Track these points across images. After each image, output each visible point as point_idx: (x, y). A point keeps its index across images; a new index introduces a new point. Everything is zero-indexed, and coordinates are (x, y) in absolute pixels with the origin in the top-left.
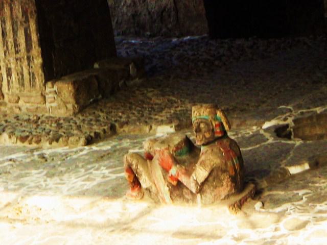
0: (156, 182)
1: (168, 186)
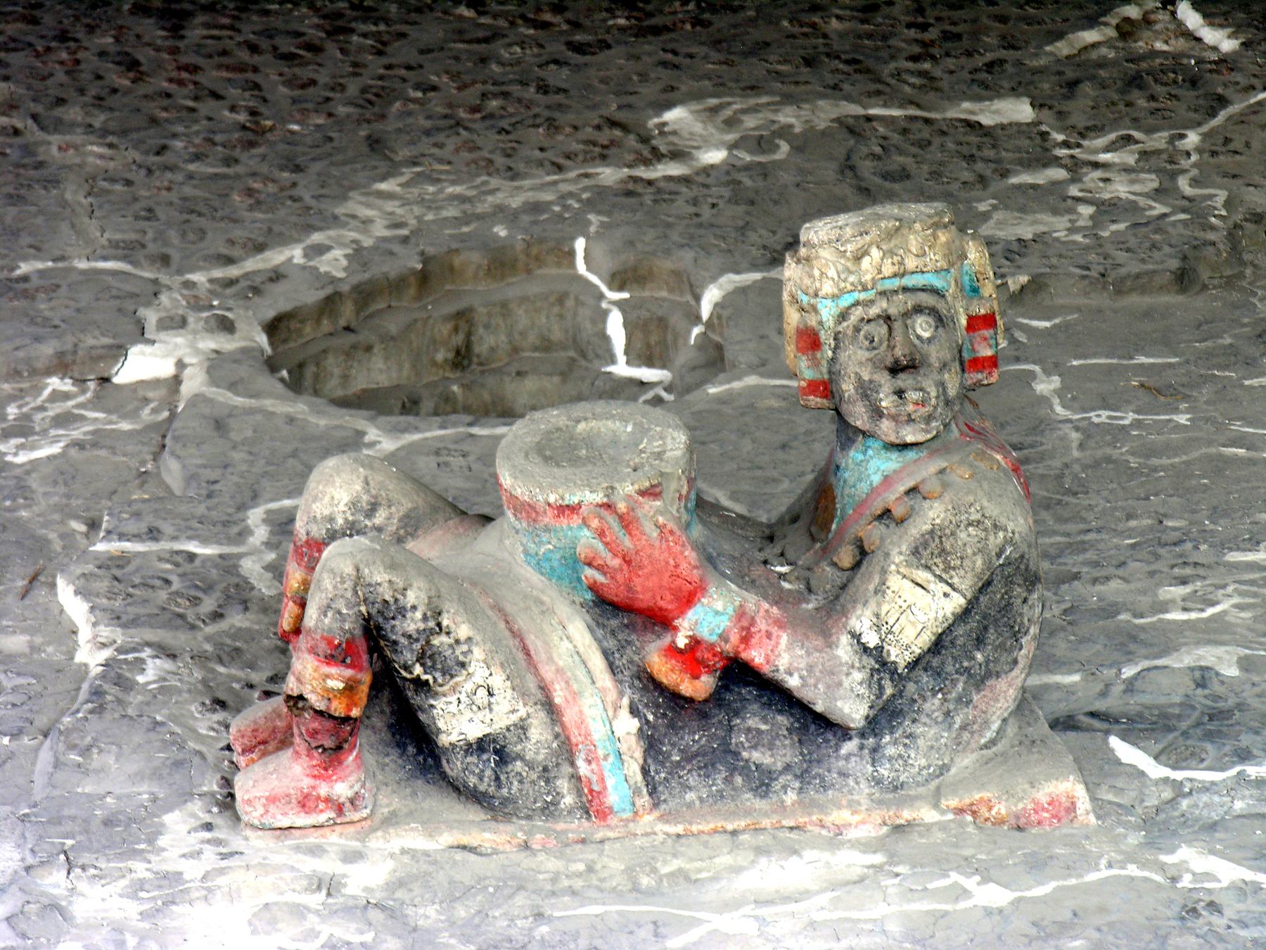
1: (634, 711)
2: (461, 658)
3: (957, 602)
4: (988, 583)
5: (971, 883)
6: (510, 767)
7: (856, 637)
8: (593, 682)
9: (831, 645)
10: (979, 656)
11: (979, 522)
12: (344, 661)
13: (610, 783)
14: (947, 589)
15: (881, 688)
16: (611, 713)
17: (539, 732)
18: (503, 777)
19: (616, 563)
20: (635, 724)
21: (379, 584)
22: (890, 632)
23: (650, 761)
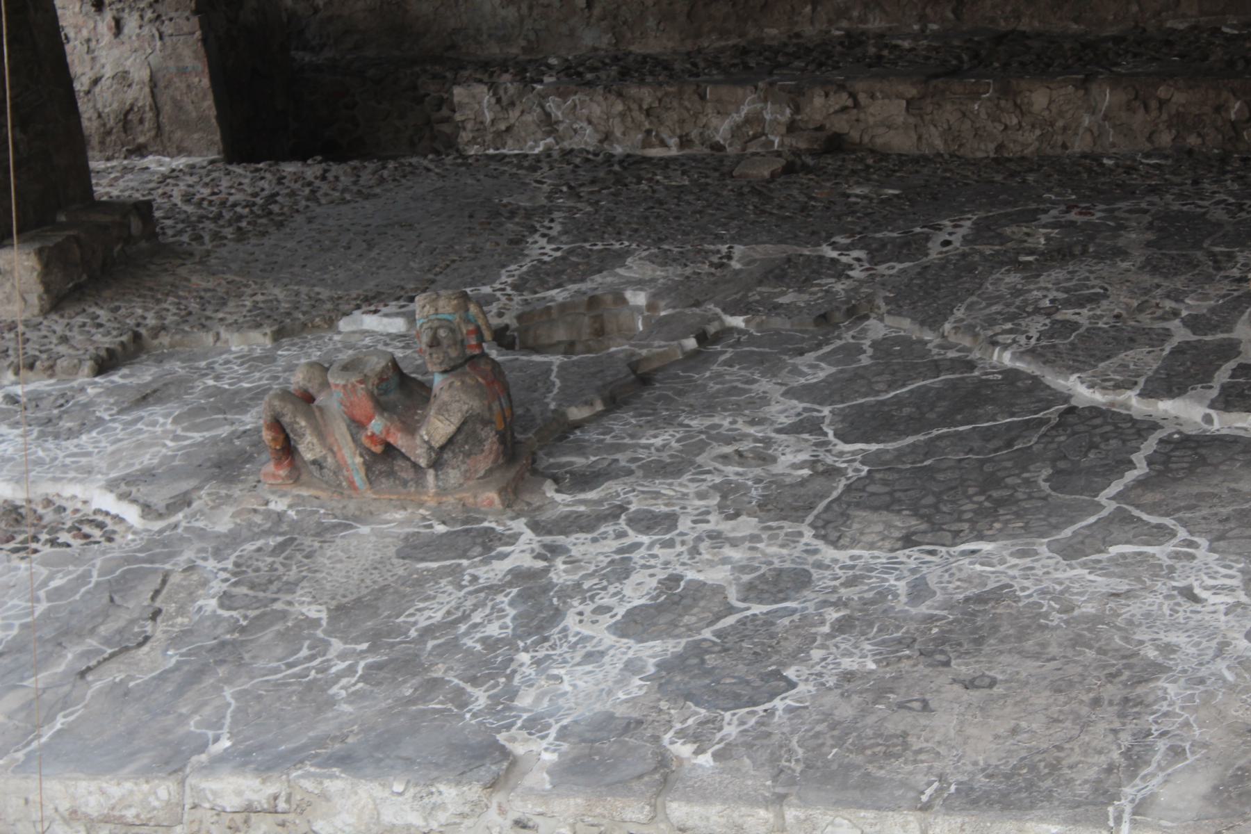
0: (335, 449)
1: (361, 455)
3: (452, 429)
4: (464, 423)
17: (330, 460)
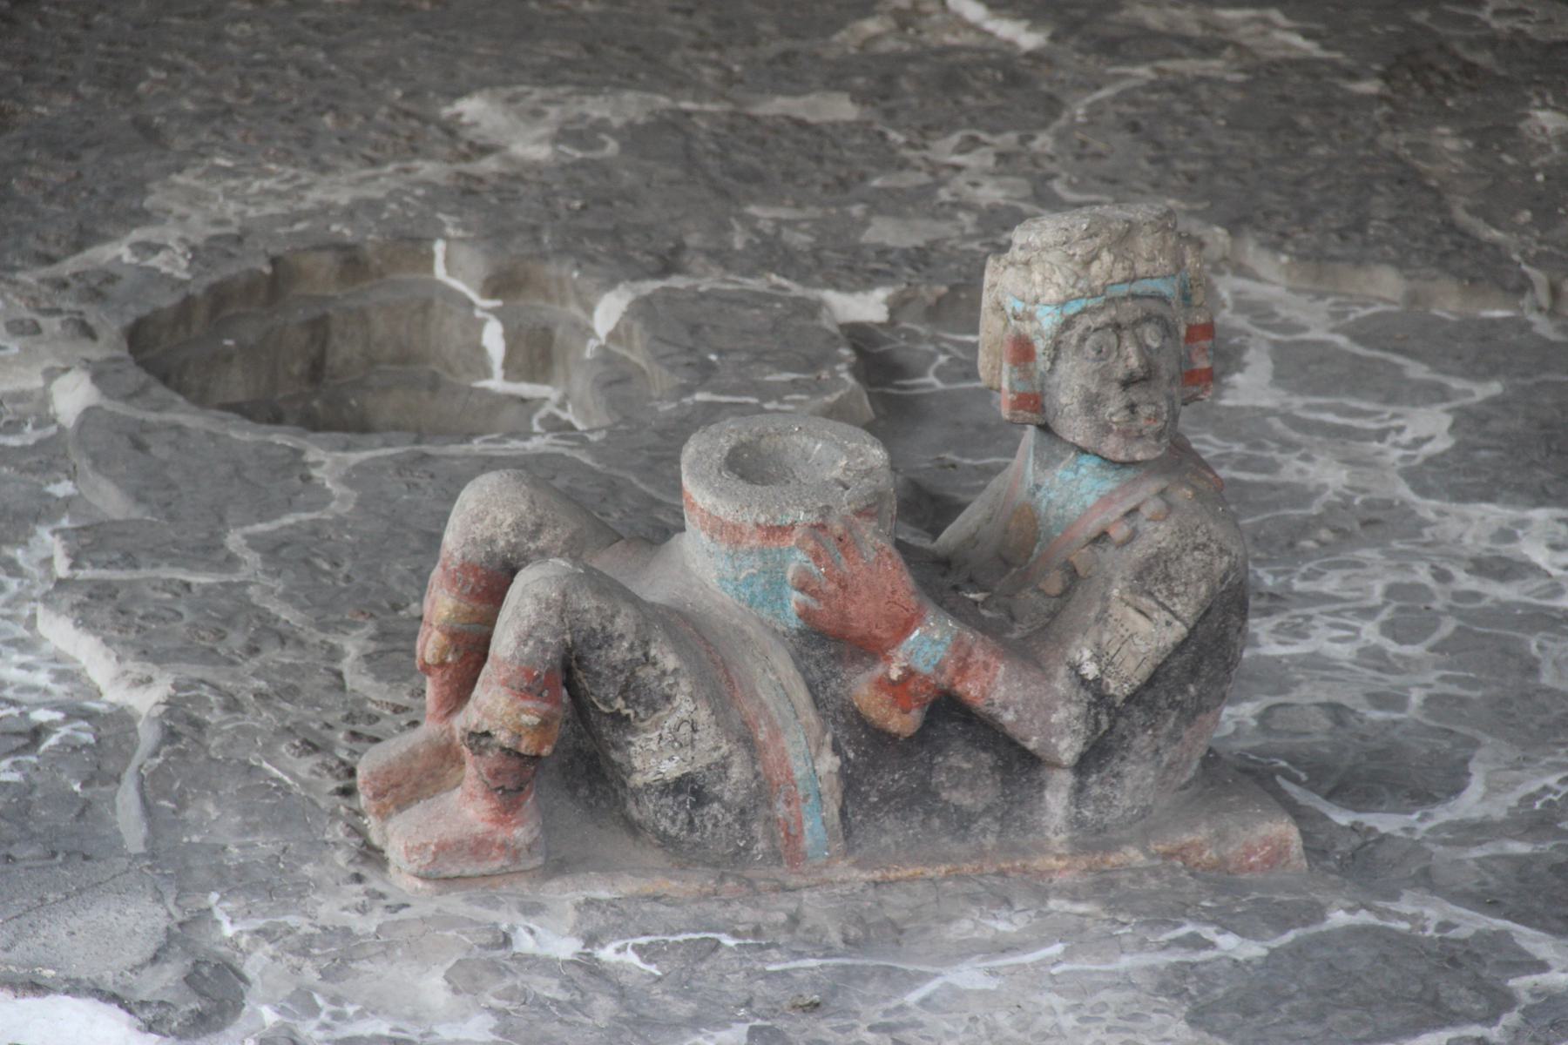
1: (836, 749)
2: (667, 690)
3: (1178, 631)
5: (1209, 932)
6: (706, 810)
7: (1075, 668)
8: (797, 717)
9: (1049, 677)
10: (1192, 689)
11: (1205, 546)
12: (540, 694)
13: (807, 825)
14: (1168, 616)
15: (1097, 723)
16: (813, 750)
17: (735, 772)
18: (697, 821)
19: (832, 587)
20: (837, 761)
21: (586, 611)
22: (1110, 663)
23: (847, 802)
